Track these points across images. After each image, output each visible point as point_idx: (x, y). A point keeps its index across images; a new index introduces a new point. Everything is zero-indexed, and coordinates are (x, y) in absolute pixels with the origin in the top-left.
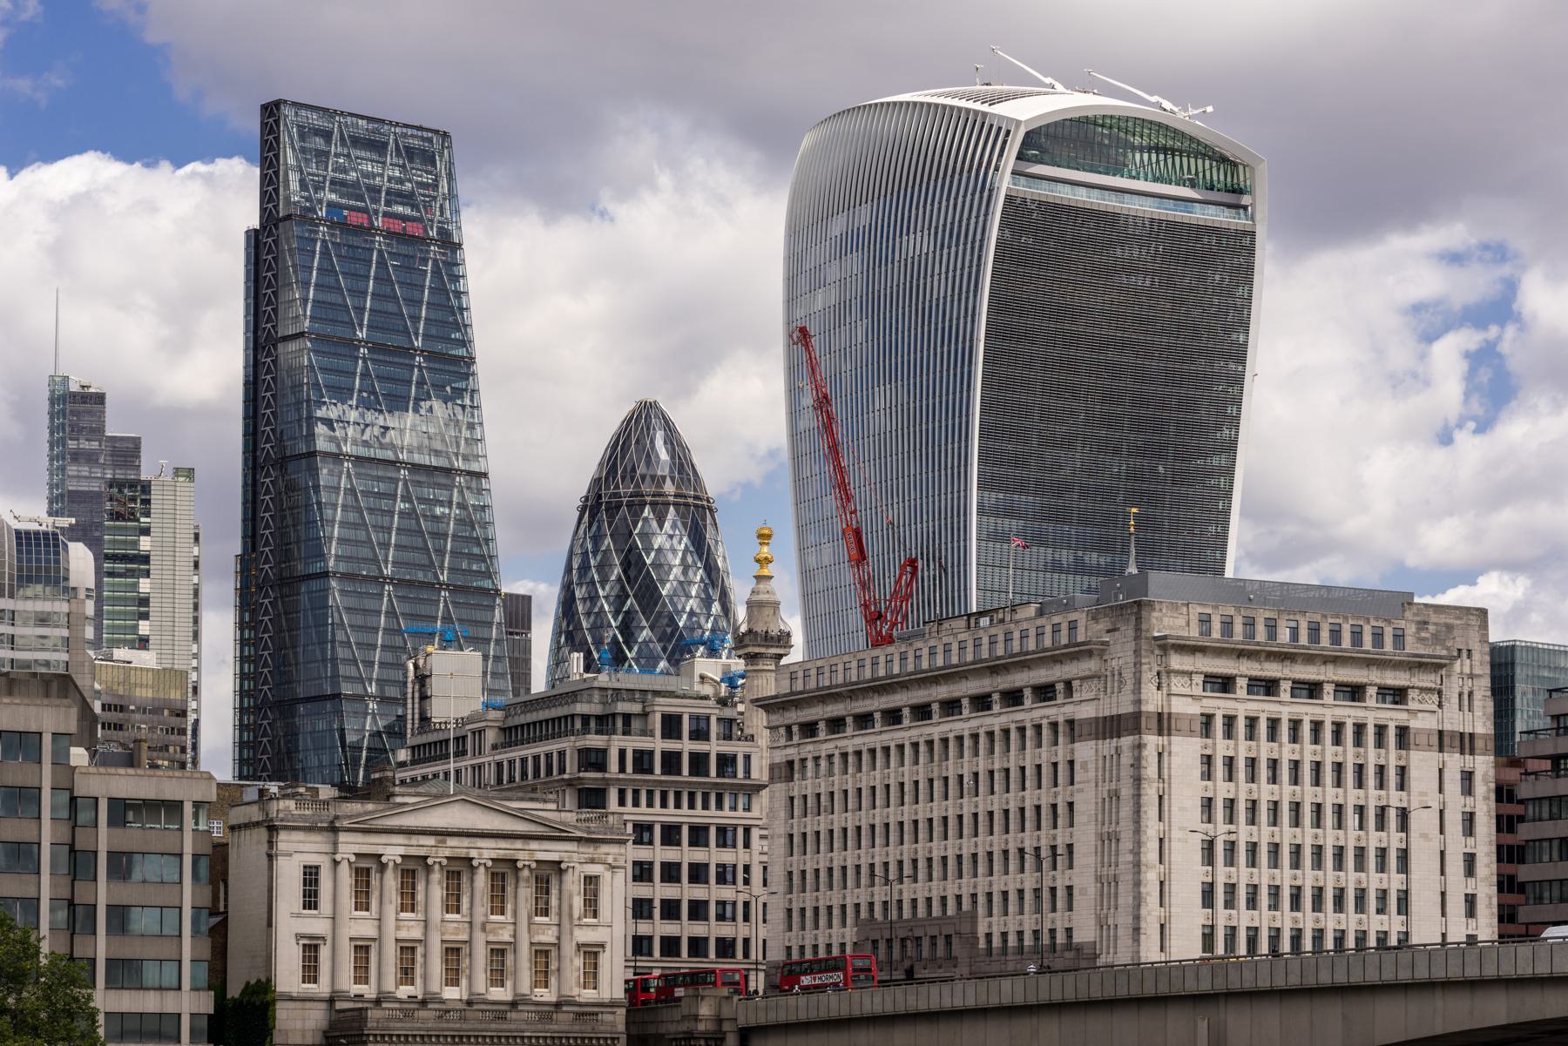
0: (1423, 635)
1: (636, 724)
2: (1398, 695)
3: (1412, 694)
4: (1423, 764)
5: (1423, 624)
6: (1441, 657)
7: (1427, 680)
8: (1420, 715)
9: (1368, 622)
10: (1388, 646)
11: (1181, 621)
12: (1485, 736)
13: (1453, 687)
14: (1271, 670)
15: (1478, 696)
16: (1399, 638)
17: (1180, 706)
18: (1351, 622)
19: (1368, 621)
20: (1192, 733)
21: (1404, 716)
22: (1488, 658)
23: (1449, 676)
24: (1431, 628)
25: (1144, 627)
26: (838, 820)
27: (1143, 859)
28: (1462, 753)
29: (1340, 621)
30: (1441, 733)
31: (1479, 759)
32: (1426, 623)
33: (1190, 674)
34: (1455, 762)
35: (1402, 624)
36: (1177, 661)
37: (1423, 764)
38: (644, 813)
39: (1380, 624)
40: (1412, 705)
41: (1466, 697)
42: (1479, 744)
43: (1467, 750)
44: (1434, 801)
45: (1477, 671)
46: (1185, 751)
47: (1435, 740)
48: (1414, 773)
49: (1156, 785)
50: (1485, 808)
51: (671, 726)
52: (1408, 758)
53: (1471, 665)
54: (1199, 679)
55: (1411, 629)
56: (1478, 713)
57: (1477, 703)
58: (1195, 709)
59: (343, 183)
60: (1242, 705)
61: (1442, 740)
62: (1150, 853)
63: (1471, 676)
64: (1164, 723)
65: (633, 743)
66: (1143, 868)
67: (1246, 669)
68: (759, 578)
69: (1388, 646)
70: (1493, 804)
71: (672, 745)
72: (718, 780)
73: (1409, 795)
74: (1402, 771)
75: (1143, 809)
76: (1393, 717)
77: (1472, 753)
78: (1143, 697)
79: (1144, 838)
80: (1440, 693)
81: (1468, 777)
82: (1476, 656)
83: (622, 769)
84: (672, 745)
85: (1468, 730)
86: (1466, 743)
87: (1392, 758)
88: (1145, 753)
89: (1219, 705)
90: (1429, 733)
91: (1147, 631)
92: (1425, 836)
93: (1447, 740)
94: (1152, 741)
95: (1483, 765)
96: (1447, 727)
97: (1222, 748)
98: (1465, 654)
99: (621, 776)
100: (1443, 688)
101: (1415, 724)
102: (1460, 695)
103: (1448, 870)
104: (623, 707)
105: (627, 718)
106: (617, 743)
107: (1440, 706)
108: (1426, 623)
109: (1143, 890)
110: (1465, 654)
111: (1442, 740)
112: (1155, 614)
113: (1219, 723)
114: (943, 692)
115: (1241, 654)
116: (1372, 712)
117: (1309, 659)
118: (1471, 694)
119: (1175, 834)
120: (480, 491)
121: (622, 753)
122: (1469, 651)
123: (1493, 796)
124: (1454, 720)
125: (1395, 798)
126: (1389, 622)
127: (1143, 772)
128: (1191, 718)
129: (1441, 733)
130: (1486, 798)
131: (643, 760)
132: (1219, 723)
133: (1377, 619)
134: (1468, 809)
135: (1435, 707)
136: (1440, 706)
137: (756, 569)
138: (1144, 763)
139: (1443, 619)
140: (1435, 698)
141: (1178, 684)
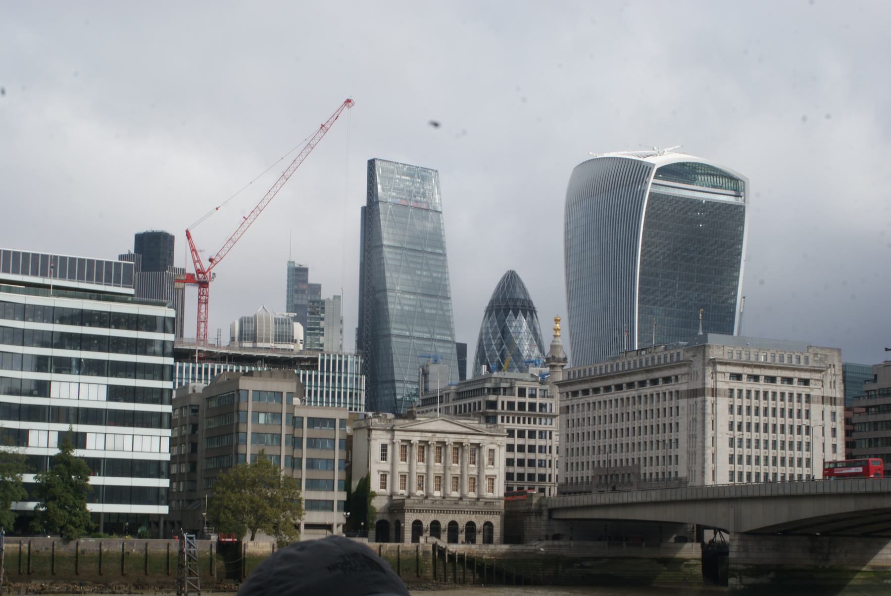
0: (816, 359)
1: (508, 391)
2: (806, 382)
3: (811, 381)
4: (816, 409)
5: (816, 355)
6: (823, 367)
7: (817, 376)
8: (815, 390)
9: (794, 353)
10: (802, 363)
11: (721, 353)
12: (840, 398)
13: (828, 379)
14: (756, 372)
15: (837, 383)
16: (807, 359)
17: (720, 386)
18: (787, 353)
19: (794, 353)
20: (725, 396)
22: (841, 368)
23: (826, 375)
24: (819, 356)
25: (706, 355)
26: (642, 423)
27: (706, 445)
28: (831, 405)
29: (783, 353)
30: (823, 397)
31: (838, 407)
32: (817, 354)
33: (724, 373)
34: (828, 408)
35: (807, 354)
36: (719, 368)
38: (511, 426)
39: (799, 354)
40: (811, 386)
41: (833, 383)
42: (838, 401)
43: (833, 403)
44: (820, 422)
45: (837, 373)
46: (723, 403)
47: (820, 400)
48: (812, 413)
50: (840, 426)
51: (522, 393)
52: (810, 407)
53: (835, 371)
54: (728, 375)
55: (811, 357)
56: (837, 389)
57: (837, 386)
58: (726, 387)
59: (398, 189)
60: (745, 385)
62: (709, 442)
63: (835, 375)
64: (715, 392)
65: (507, 399)
66: (706, 448)
69: (802, 363)
70: (843, 425)
71: (522, 400)
72: (540, 413)
73: (810, 421)
74: (808, 412)
75: (706, 425)
76: (804, 390)
77: (835, 405)
78: (706, 382)
79: (706, 437)
80: (822, 381)
81: (834, 414)
82: (837, 367)
83: (503, 408)
84: (522, 400)
85: (834, 396)
86: (833, 401)
87: (804, 407)
88: (707, 404)
89: (736, 385)
90: (818, 397)
91: (708, 356)
92: (816, 437)
93: (825, 400)
94: (709, 399)
95: (839, 409)
96: (825, 395)
98: (832, 366)
99: (502, 411)
100: (824, 379)
101: (812, 393)
102: (830, 382)
103: (826, 450)
104: (503, 385)
105: (505, 389)
106: (502, 399)
107: (823, 386)
108: (817, 354)
109: (706, 457)
110: (832, 366)
112: (711, 350)
113: (736, 393)
114: (627, 379)
116: (796, 388)
117: (771, 368)
118: (834, 382)
119: (719, 435)
120: (448, 304)
121: (503, 403)
122: (834, 365)
123: (843, 422)
124: (828, 392)
125: (805, 422)
126: (802, 353)
127: (706, 411)
128: (725, 390)
129: (823, 397)
130: (841, 423)
131: (511, 405)
132: (736, 393)
133: (798, 352)
134: (834, 427)
135: (820, 387)
136: (823, 386)
137: (554, 333)
138: (706, 408)
140: (821, 383)
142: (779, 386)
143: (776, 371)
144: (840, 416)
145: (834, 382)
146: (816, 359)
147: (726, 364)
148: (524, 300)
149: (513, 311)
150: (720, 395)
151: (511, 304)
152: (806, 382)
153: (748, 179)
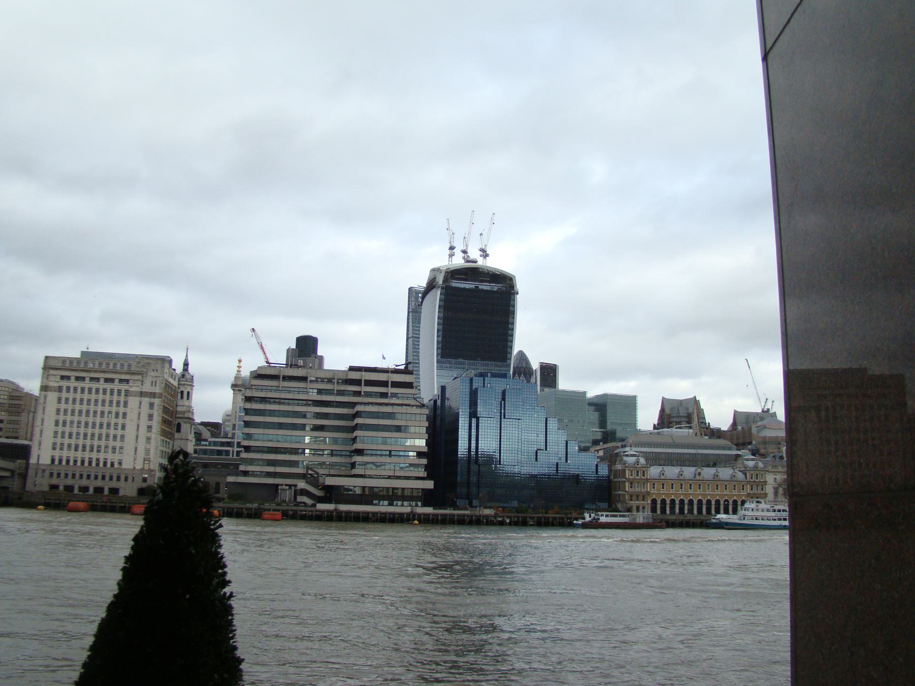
0: (139, 365)
3: (131, 381)
8: (134, 387)
9: (119, 361)
15: (158, 382)
21: (128, 387)
31: (156, 399)
33: (55, 375)
34: (146, 401)
37: (133, 402)
40: (130, 384)
42: (157, 395)
44: (136, 411)
48: (129, 403)
49: (42, 405)
50: (157, 413)
54: (59, 377)
56: (157, 387)
57: (157, 384)
60: (73, 384)
61: (142, 394)
67: (73, 374)
68: (238, 371)
76: (124, 387)
80: (143, 381)
81: (152, 405)
86: (153, 395)
89: (65, 384)
97: (64, 395)
98: (155, 371)
102: (152, 382)
110: (155, 371)
111: (142, 394)
115: (72, 370)
117: (96, 372)
118: (156, 382)
124: (147, 388)
126: (127, 362)
135: (140, 385)
136: (142, 385)
137: (237, 368)
139: (146, 361)
140: (140, 383)
141: (51, 378)
142: (117, 385)
143: (100, 374)
144: (158, 405)
145: (156, 382)
146: (139, 365)
147: (57, 369)
148: (521, 367)
149: (518, 374)
150: (51, 391)
151: (522, 370)
152: (127, 381)
153: (515, 276)
